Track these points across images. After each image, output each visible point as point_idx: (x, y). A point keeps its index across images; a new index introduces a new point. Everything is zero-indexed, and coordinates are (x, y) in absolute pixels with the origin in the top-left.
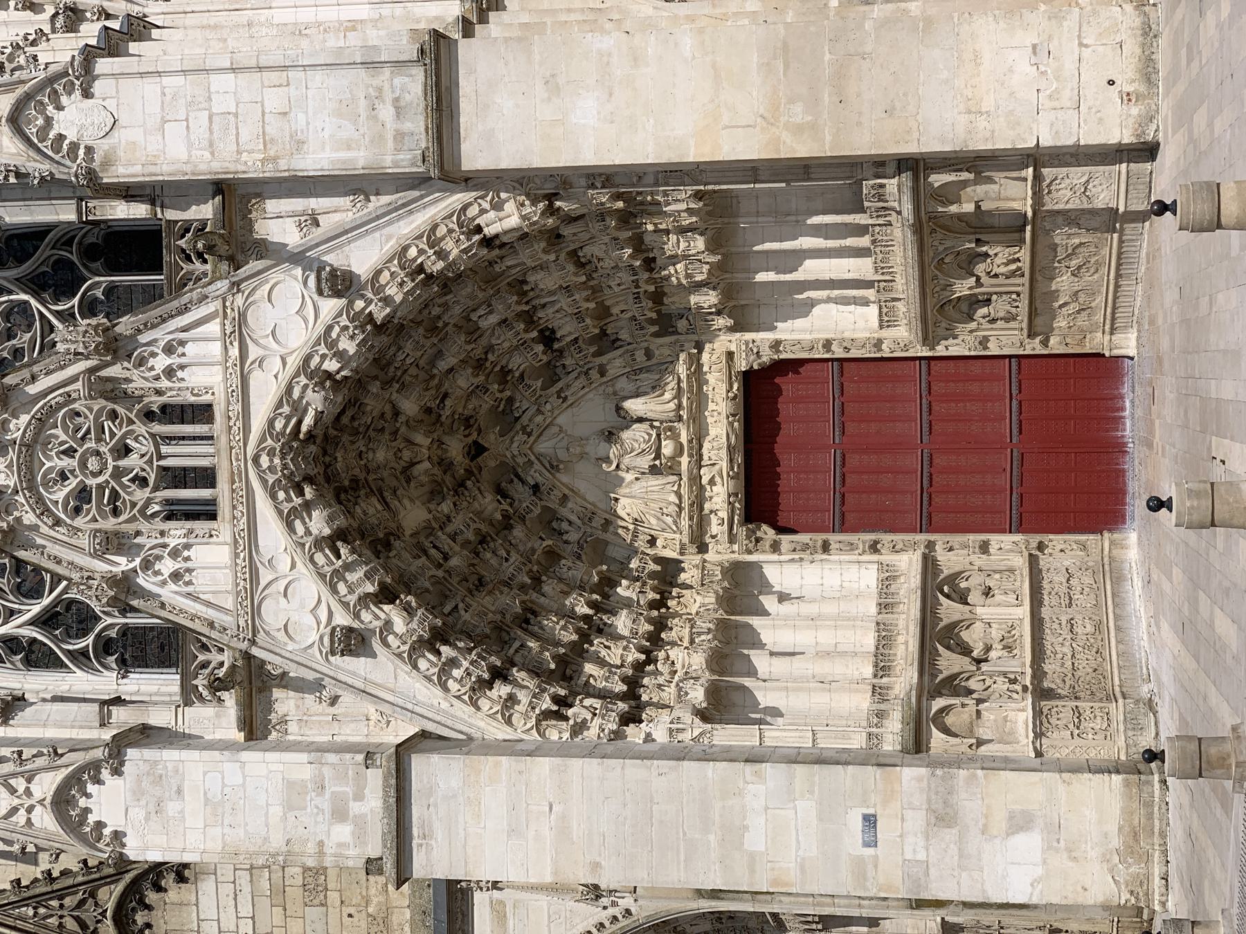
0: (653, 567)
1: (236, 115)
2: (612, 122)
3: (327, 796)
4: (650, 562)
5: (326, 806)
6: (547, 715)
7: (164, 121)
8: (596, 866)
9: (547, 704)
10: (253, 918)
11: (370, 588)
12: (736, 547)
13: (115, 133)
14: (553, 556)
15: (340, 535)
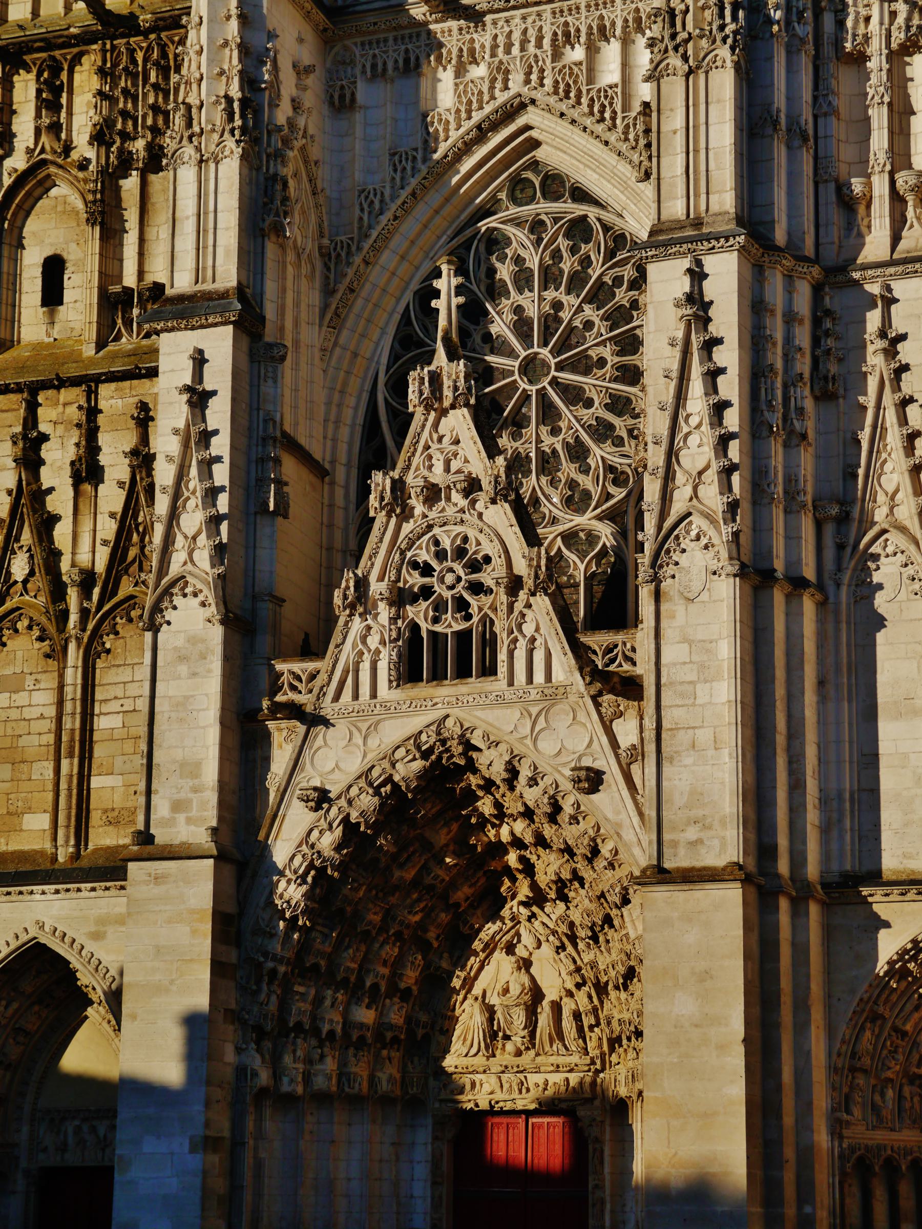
0: (420, 1032)
1: (694, 705)
2: (676, 1027)
3: (191, 795)
4: (424, 1031)
5: (182, 795)
6: (260, 965)
7: (690, 643)
8: (134, 1017)
9: (270, 965)
10: (134, 710)
11: (354, 816)
12: (437, 1105)
13: (682, 601)
14: (424, 947)
15: (396, 786)
